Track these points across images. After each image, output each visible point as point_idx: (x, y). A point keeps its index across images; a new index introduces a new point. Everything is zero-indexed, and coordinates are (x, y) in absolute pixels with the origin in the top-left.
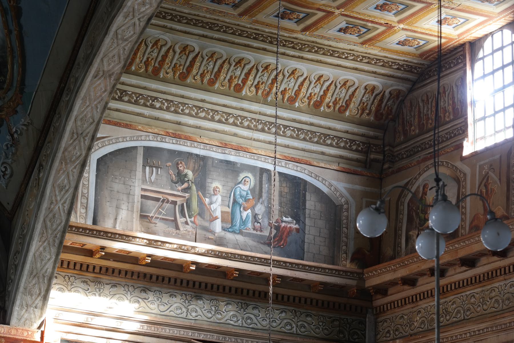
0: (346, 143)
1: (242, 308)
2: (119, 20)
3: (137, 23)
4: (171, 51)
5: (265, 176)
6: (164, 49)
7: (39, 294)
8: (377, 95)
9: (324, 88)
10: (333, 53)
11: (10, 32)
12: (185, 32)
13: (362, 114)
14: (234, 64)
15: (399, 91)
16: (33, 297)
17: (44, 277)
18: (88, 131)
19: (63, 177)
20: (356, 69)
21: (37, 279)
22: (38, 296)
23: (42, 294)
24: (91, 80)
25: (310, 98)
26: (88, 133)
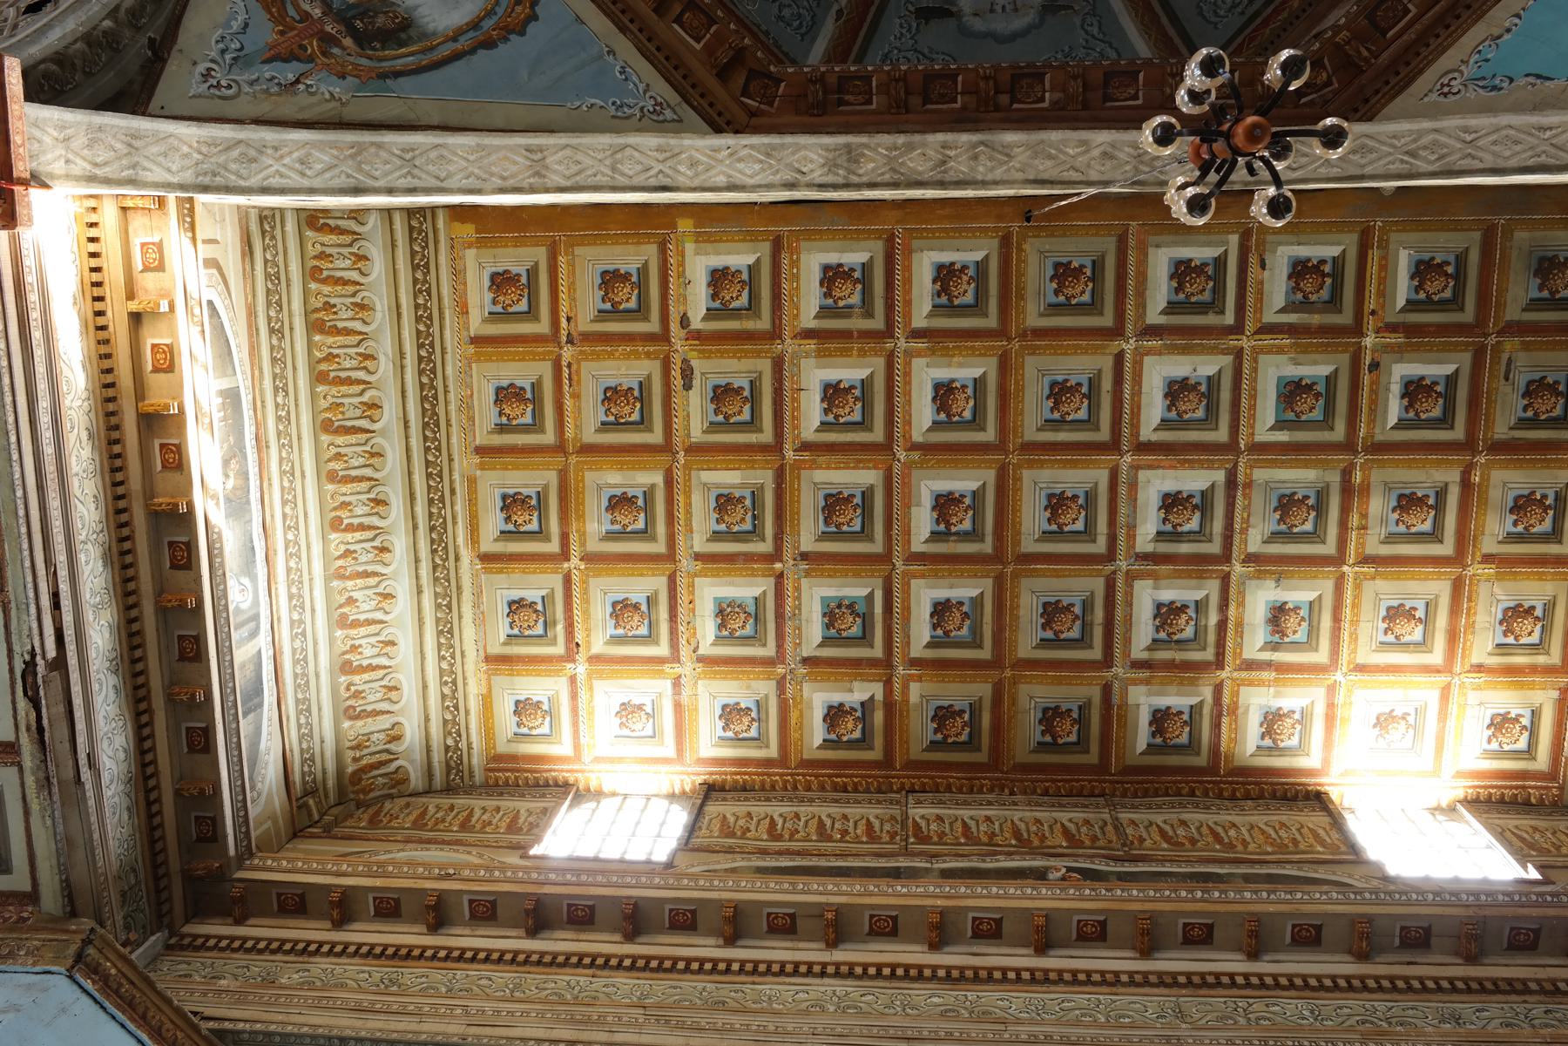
0: (309, 748)
1: (111, 661)
2: (650, 141)
3: (652, 172)
4: (362, 387)
5: (252, 625)
6: (361, 375)
7: (96, 165)
8: (387, 751)
9: (375, 662)
10: (446, 631)
11: (455, 39)
12: (403, 392)
13: (352, 748)
14: (372, 496)
15: (406, 780)
16: (86, 151)
17: (134, 166)
18: (424, 176)
19: (326, 158)
20: (425, 687)
21: (126, 151)
22: (90, 163)
23: (98, 172)
24: (520, 146)
25: (354, 648)
26: (420, 178)
